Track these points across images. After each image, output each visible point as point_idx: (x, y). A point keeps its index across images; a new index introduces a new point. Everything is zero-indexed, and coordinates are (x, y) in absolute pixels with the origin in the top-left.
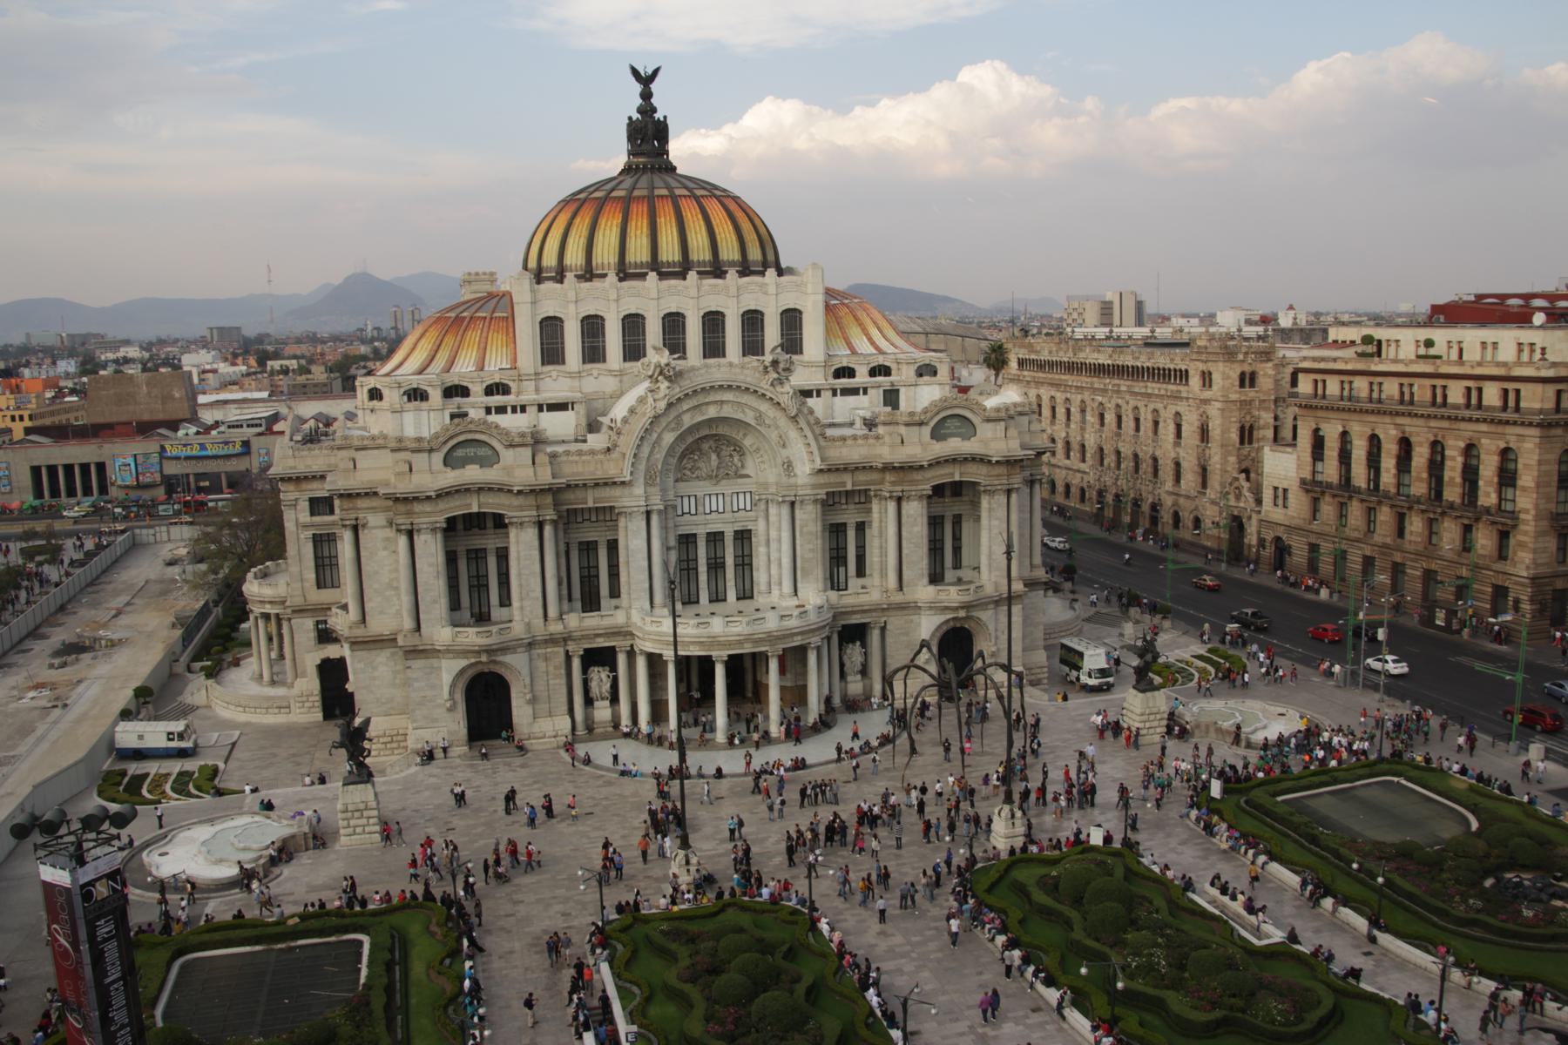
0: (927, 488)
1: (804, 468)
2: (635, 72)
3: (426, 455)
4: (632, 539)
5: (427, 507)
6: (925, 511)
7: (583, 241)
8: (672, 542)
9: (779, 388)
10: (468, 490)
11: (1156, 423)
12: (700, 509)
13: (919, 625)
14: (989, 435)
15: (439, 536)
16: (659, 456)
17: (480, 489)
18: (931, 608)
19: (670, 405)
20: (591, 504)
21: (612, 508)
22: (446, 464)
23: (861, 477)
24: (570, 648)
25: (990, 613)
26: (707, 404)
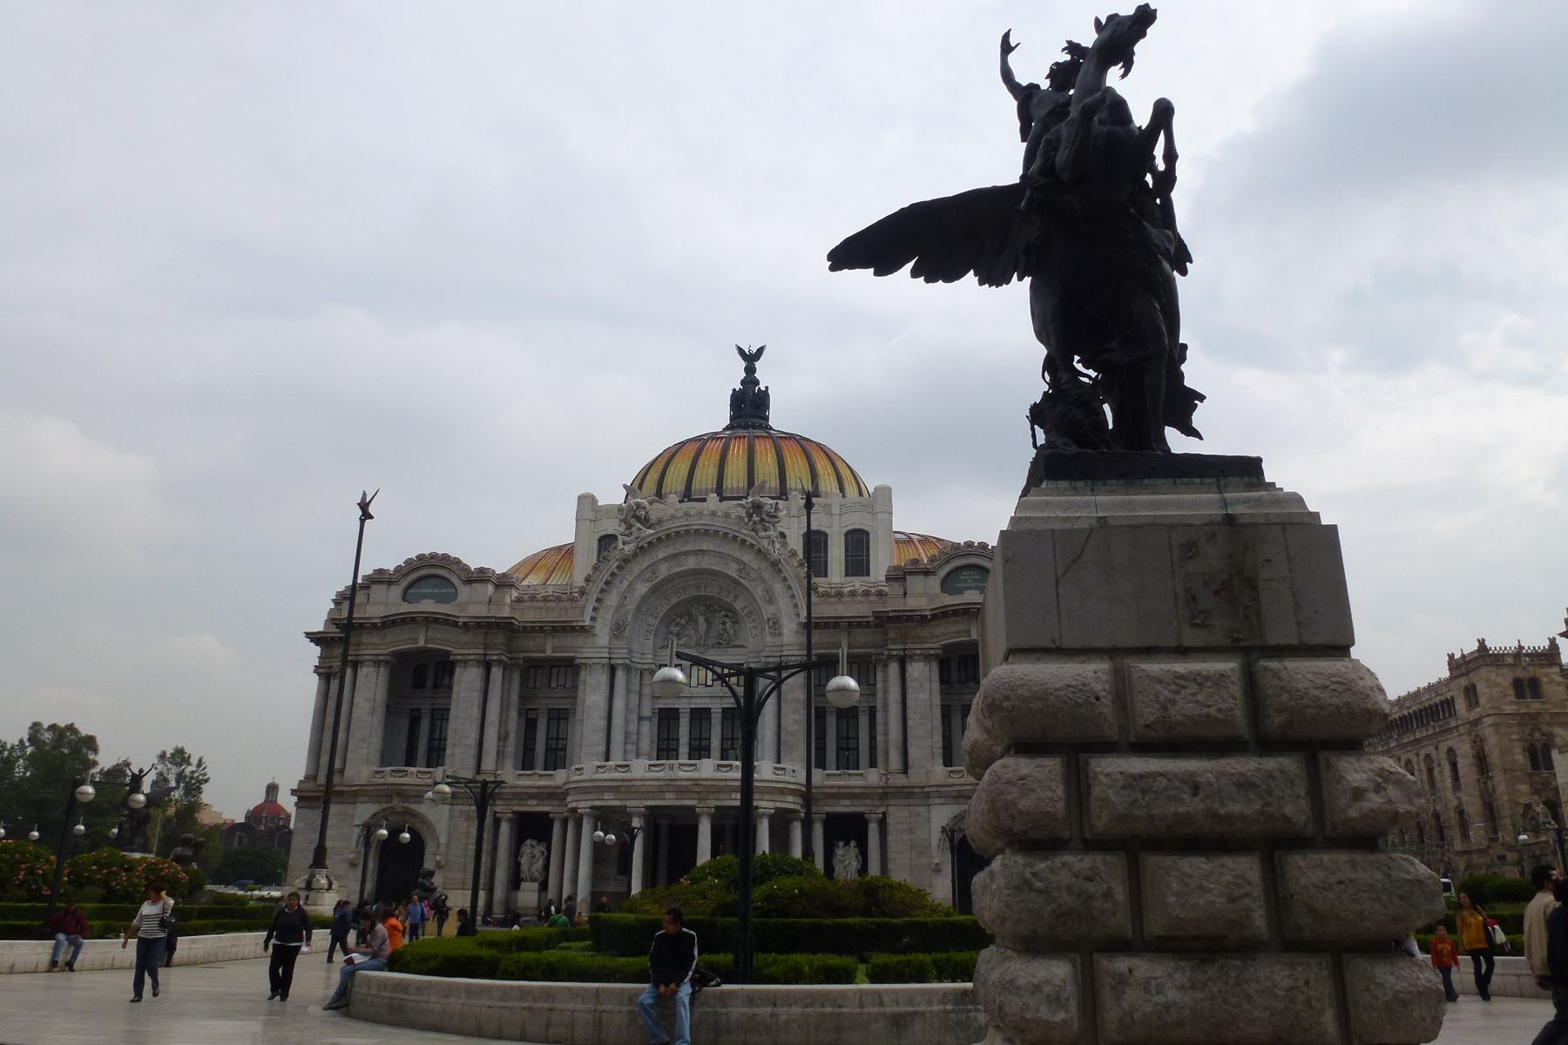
0: (935, 646)
2: (741, 351)
5: (375, 638)
6: (936, 675)
8: (646, 712)
9: (763, 534)
10: (413, 619)
11: (1430, 771)
15: (383, 672)
16: (631, 605)
19: (641, 550)
20: (549, 653)
21: (573, 659)
22: (404, 599)
23: (861, 637)
24: (498, 809)
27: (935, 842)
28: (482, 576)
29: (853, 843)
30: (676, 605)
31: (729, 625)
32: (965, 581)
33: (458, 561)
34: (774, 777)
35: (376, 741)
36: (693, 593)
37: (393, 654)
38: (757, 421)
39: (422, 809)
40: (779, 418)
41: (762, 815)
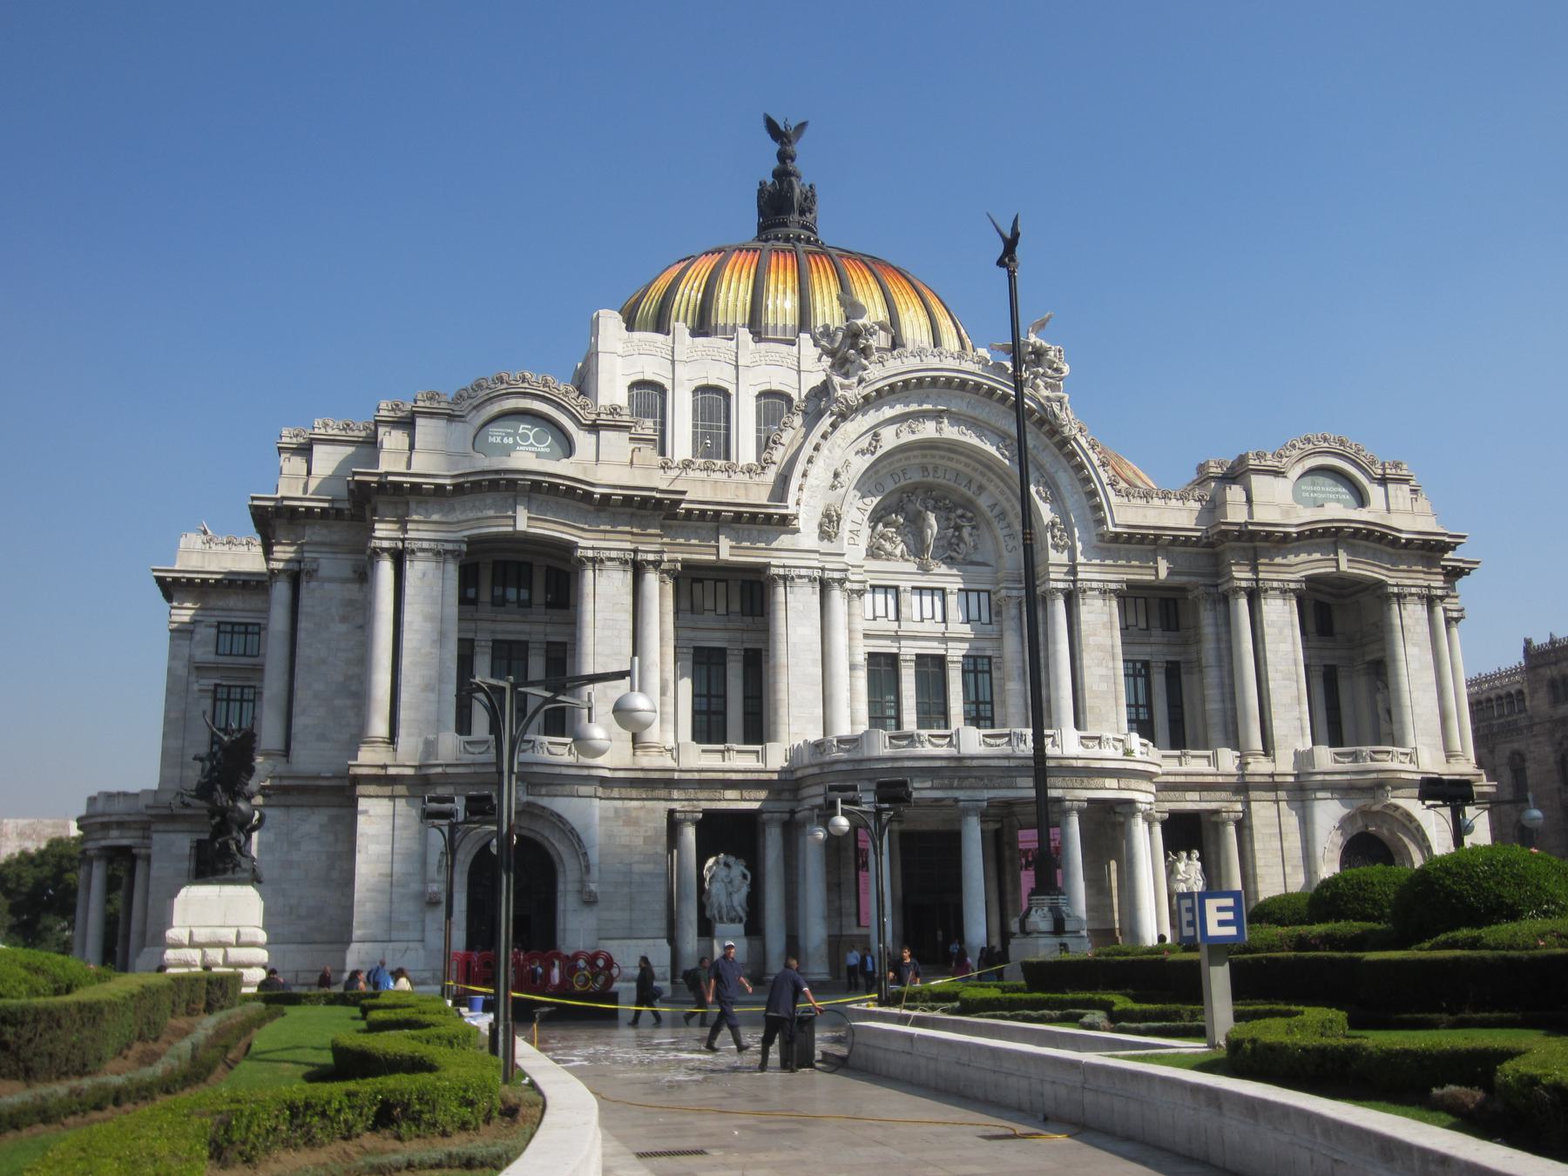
2: (772, 127)
8: (861, 659)
10: (512, 484)
12: (904, 609)
15: (452, 569)
17: (536, 486)
18: (1324, 787)
24: (676, 806)
29: (1196, 854)
31: (966, 532)
36: (916, 477)
38: (804, 234)
39: (561, 805)
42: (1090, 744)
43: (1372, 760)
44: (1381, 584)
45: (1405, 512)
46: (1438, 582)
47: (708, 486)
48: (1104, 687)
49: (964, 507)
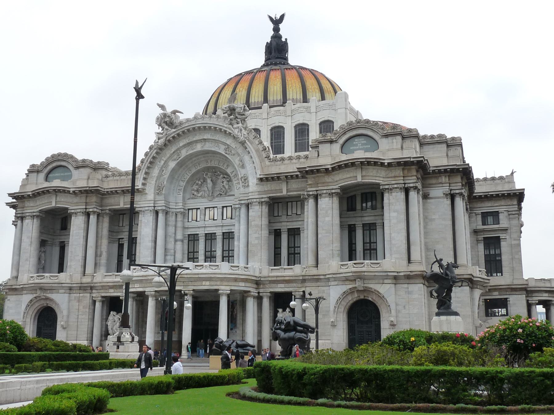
0: (335, 187)
1: (253, 181)
2: (271, 18)
3: (36, 174)
4: (145, 228)
7: (216, 98)
8: (179, 236)
10: (48, 191)
13: (329, 295)
14: (387, 148)
18: (335, 279)
22: (46, 179)
23: (295, 185)
24: (94, 295)
25: (388, 286)
26: (197, 142)
27: (332, 308)
28: (84, 165)
30: (198, 172)
31: (225, 182)
32: (356, 145)
33: (72, 157)
34: (231, 272)
35: (33, 260)
36: (203, 165)
37: (41, 211)
38: (283, 61)
40: (293, 59)
41: (223, 294)
42: (199, 268)
43: (354, 267)
44: (378, 185)
45: (397, 149)
46: (412, 180)
47: (119, 183)
48: (256, 242)
49: (223, 174)
